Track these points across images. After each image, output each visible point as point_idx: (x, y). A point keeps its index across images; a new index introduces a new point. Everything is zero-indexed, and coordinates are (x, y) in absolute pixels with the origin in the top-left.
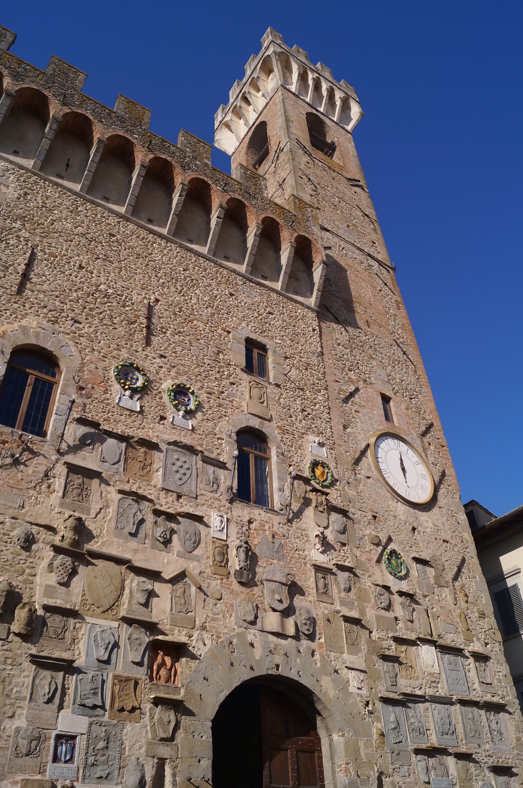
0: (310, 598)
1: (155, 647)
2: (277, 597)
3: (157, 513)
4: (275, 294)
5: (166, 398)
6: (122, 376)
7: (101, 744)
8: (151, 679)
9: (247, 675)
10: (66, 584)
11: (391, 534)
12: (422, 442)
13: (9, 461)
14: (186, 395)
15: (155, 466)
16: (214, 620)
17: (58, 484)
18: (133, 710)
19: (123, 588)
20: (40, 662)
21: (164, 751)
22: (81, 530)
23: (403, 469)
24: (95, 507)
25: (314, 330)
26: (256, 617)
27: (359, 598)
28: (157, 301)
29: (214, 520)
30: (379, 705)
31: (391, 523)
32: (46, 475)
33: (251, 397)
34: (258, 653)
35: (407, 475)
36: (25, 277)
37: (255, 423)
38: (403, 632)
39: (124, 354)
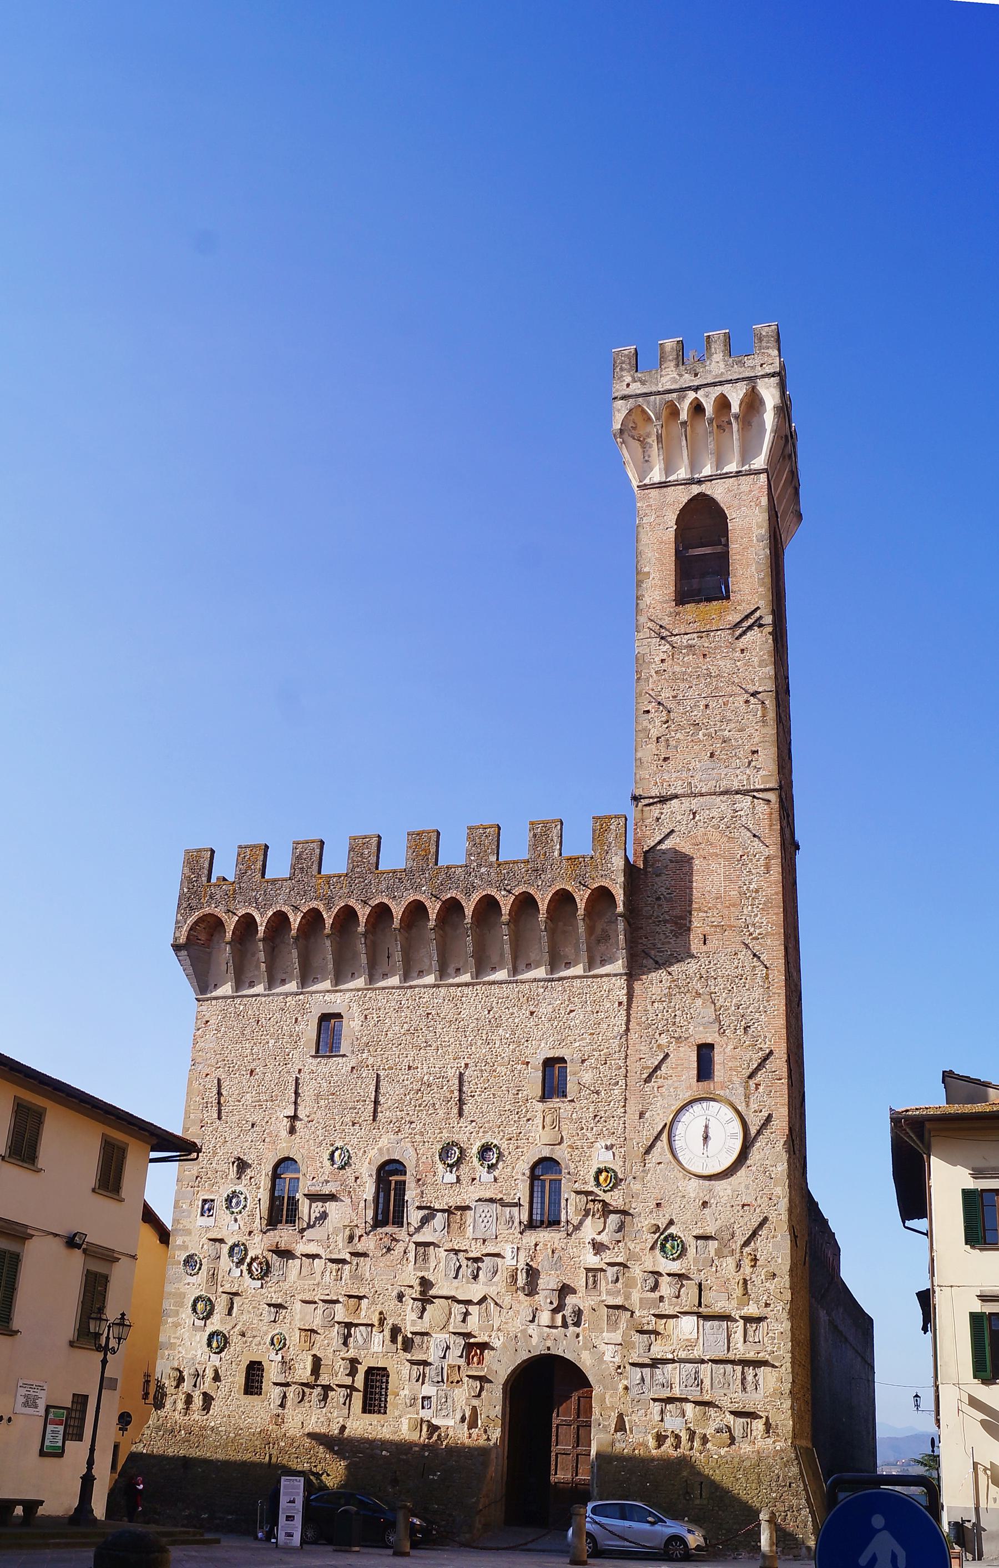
0: (580, 1295)
1: (469, 1347)
2: (549, 1301)
3: (468, 1259)
4: (579, 981)
5: (475, 1160)
6: (444, 1155)
7: (444, 1400)
8: (468, 1364)
9: (525, 1356)
10: (421, 1317)
11: (673, 1217)
12: (747, 1088)
13: (385, 1250)
14: (490, 1150)
15: (468, 1223)
16: (506, 1323)
17: (411, 1255)
18: (458, 1382)
19: (450, 1313)
20: (412, 1363)
21: (475, 1402)
22: (425, 1284)
23: (706, 1138)
24: (433, 1265)
25: (620, 1004)
26: (534, 1317)
27: (626, 1285)
28: (467, 1065)
29: (508, 1251)
30: (628, 1366)
31: (677, 1206)
32: (405, 1252)
33: (544, 1127)
34: (534, 1341)
35: (710, 1143)
36: (376, 1102)
37: (546, 1153)
38: (666, 1308)
39: (445, 1134)
